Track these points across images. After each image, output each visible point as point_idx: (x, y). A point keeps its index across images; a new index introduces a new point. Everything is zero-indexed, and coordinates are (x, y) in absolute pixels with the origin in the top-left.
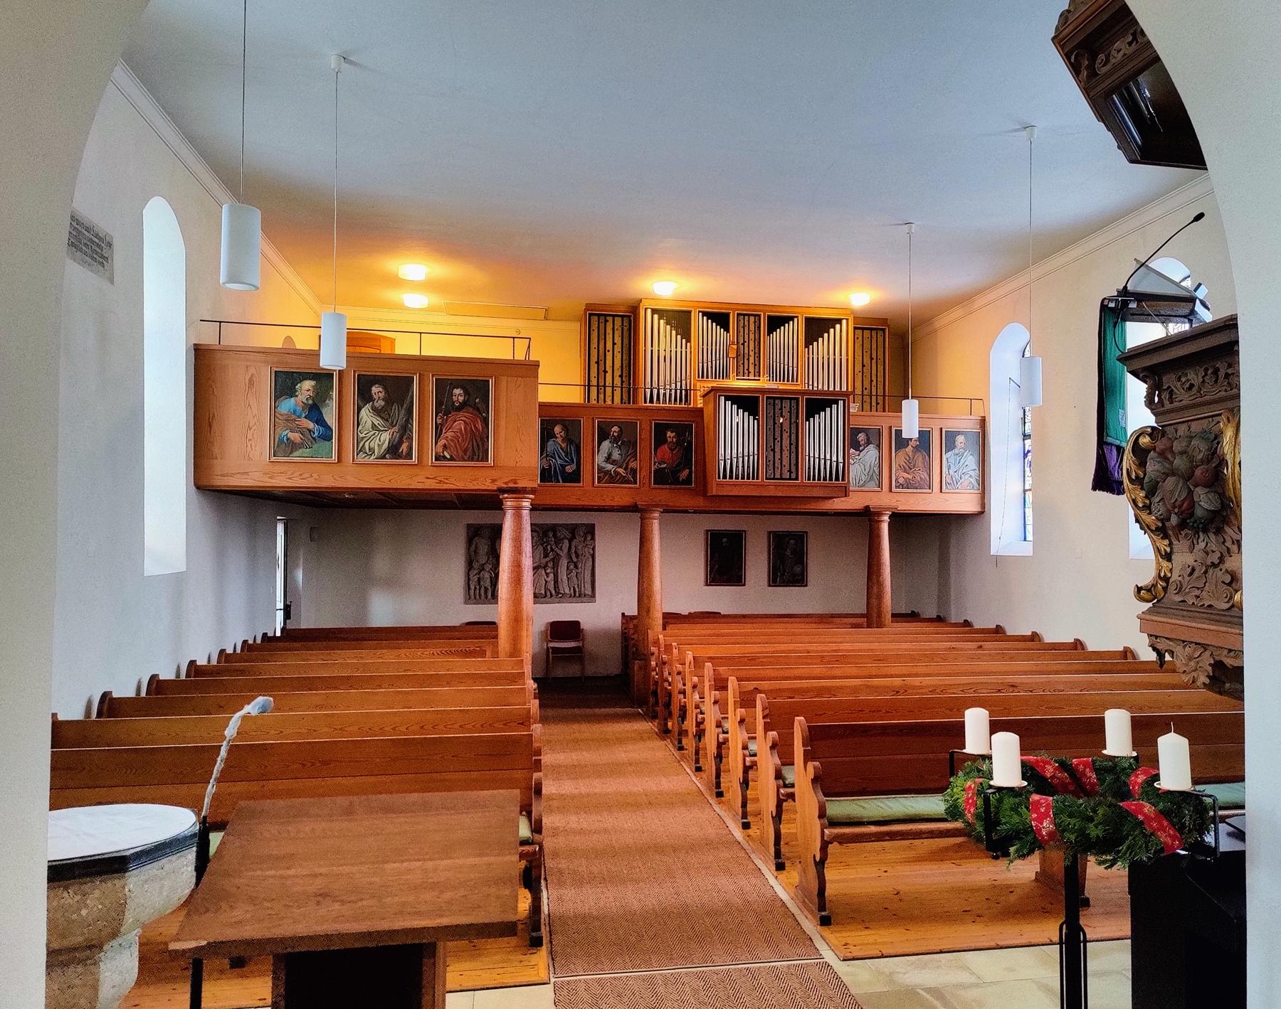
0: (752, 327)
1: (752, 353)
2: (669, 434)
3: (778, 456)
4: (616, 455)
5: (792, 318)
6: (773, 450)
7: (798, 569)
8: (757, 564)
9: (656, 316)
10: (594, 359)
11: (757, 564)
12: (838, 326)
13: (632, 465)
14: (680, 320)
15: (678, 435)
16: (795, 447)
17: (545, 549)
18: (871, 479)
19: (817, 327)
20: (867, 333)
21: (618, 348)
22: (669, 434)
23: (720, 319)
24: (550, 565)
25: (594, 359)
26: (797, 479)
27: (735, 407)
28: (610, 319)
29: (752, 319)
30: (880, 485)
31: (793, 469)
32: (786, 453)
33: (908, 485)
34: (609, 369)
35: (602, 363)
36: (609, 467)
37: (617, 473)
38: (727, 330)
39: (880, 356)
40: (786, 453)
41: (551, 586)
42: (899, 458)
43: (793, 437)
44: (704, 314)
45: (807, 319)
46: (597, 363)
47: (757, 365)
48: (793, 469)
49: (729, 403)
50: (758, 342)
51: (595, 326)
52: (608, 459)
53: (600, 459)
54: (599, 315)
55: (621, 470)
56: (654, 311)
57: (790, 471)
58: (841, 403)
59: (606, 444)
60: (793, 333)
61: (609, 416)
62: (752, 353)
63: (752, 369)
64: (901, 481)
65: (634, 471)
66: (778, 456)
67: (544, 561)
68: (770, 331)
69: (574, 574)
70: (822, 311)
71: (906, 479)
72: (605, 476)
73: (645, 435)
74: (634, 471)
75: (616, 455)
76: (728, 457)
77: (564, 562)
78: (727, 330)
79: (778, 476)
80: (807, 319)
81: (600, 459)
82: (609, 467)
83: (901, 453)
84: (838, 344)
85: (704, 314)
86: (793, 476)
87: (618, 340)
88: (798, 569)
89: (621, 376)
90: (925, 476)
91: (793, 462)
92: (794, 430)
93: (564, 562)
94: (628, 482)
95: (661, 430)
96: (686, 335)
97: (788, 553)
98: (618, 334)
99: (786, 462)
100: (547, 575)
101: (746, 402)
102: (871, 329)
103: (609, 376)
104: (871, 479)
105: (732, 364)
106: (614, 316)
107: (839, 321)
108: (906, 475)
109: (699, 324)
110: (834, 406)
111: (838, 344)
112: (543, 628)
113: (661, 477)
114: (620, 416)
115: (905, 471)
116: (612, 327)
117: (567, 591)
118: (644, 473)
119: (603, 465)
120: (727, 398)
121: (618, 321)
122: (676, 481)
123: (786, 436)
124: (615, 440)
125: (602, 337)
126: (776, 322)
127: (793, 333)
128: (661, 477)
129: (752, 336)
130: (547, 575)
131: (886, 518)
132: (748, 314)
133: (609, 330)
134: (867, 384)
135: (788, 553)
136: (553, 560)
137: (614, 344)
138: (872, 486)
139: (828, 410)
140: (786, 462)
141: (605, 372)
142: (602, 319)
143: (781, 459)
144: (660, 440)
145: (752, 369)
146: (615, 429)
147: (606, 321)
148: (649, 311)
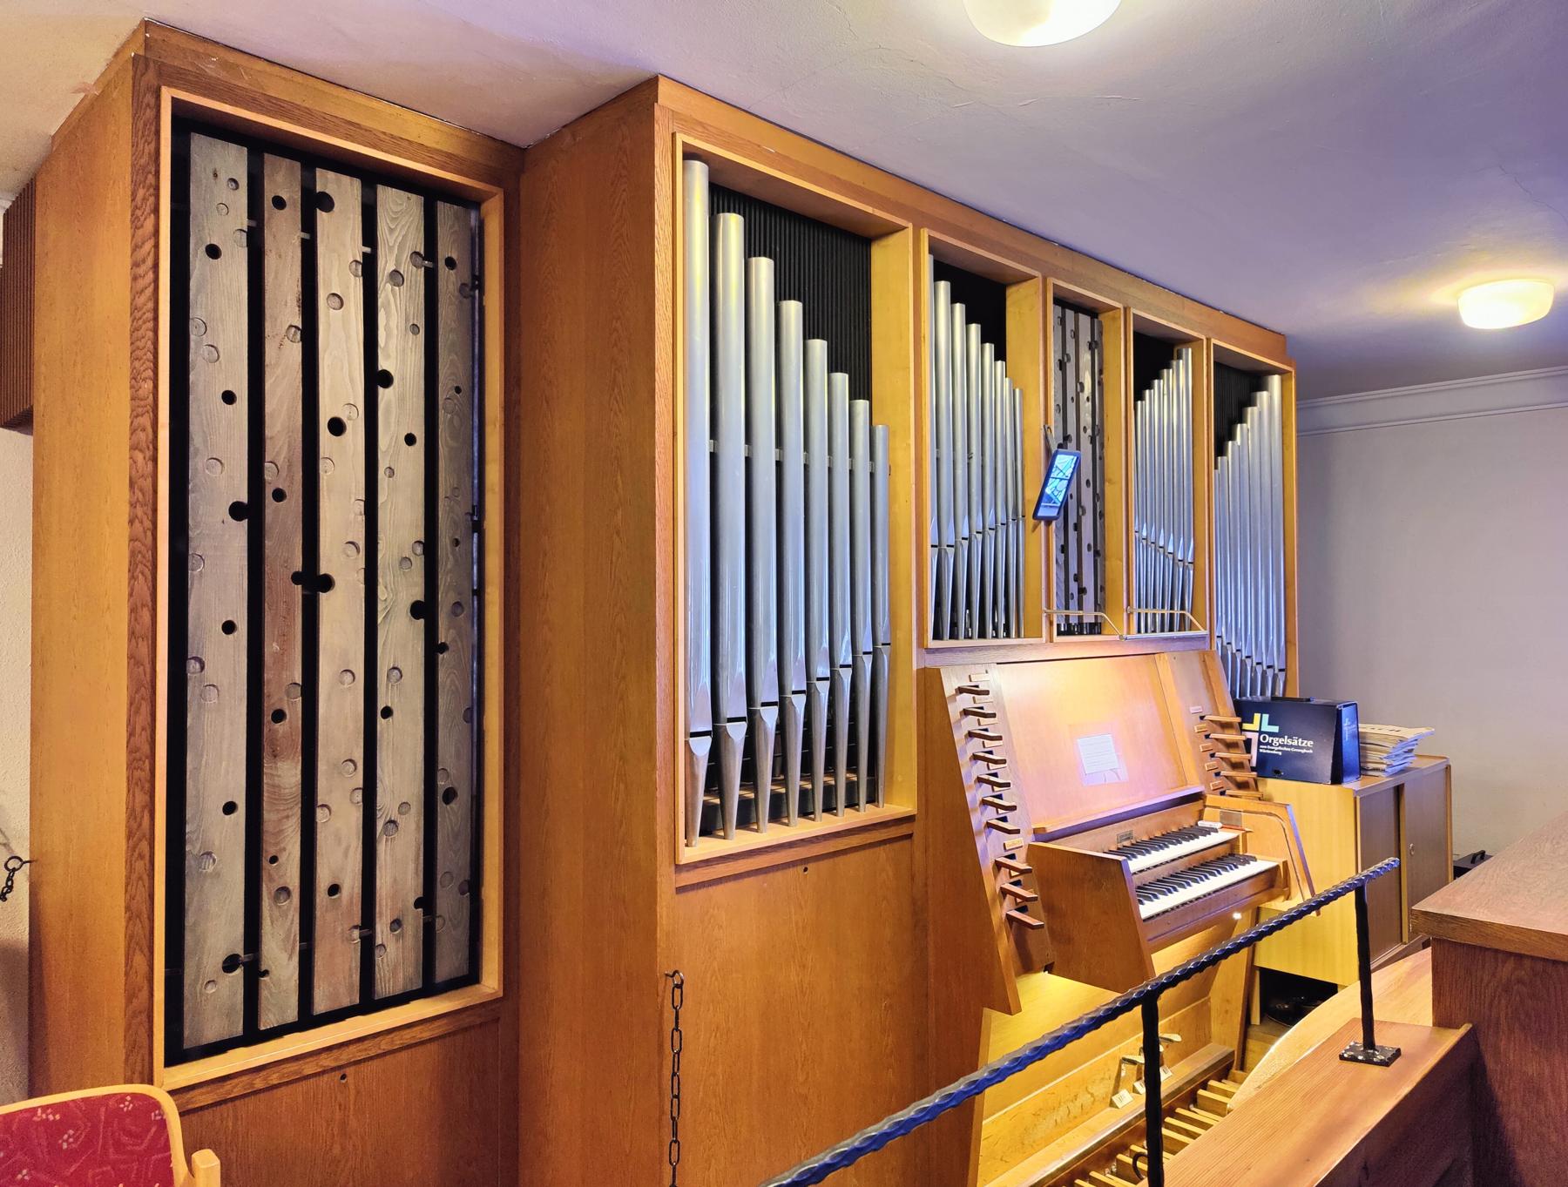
9: (733, 224)
21: (401, 409)
25: (221, 477)
34: (339, 556)
35: (283, 518)
51: (221, 215)
54: (261, 145)
87: (401, 354)
98: (399, 309)
103: (340, 615)
105: (1038, 551)
106: (372, 175)
121: (400, 217)
133: (338, 274)
137: (376, 379)
141: (314, 582)
147: (314, 203)
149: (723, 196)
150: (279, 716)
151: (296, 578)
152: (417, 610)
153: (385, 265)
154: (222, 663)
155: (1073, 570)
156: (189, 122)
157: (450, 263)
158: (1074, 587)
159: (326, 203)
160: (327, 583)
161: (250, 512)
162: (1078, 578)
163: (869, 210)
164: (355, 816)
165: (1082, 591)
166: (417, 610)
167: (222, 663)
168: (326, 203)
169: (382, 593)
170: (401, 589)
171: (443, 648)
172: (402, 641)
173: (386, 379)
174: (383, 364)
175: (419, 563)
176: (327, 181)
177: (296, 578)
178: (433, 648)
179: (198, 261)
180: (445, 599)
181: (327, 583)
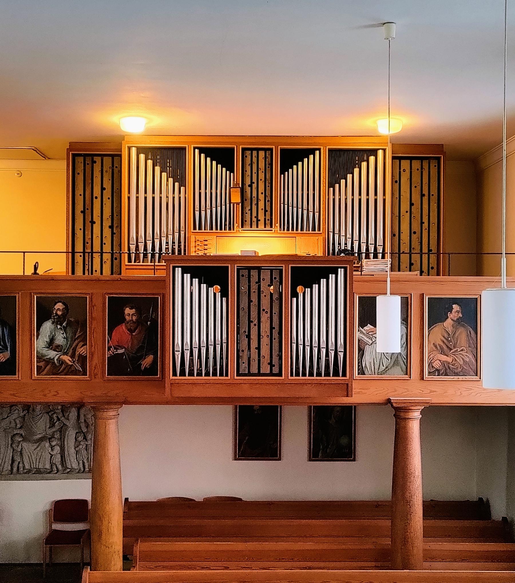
0: (262, 165)
1: (261, 197)
2: (127, 311)
3: (254, 344)
4: (60, 339)
5: (312, 151)
6: (249, 336)
7: (344, 441)
8: (295, 433)
10: (80, 207)
11: (295, 433)
12: (372, 159)
13: (81, 350)
14: (170, 158)
15: (139, 312)
16: (278, 332)
17: (51, 418)
18: (396, 363)
19: (344, 160)
20: (405, 164)
22: (127, 311)
23: (221, 155)
24: (57, 436)
25: (80, 207)
26: (280, 374)
27: (196, 281)
28: (98, 159)
29: (262, 154)
30: (407, 372)
31: (275, 361)
32: (265, 341)
33: (446, 370)
35: (88, 212)
36: (52, 354)
37: (62, 362)
38: (230, 168)
39: (434, 191)
40: (265, 341)
41: (57, 459)
42: (436, 335)
43: (276, 318)
44: (202, 150)
45: (330, 151)
46: (83, 212)
47: (269, 210)
48: (275, 361)
49: (187, 277)
50: (269, 182)
52: (51, 344)
53: (40, 344)
54: (85, 156)
55: (66, 358)
56: (140, 150)
57: (271, 365)
58: (341, 272)
59: (48, 326)
60: (315, 167)
61: (49, 290)
62: (261, 197)
63: (261, 217)
64: (437, 365)
65: (83, 360)
66: (254, 344)
67: (50, 432)
68: (284, 169)
69: (82, 447)
70: (345, 140)
71: (443, 363)
72: (47, 366)
73: (98, 314)
74: (83, 360)
75: (60, 339)
76: (187, 346)
77: (71, 434)
78: (232, 170)
79: (254, 369)
80: (330, 151)
81: (40, 344)
82: (52, 354)
83: (438, 329)
84: (374, 177)
85: (202, 150)
86: (276, 370)
88: (344, 441)
89: (111, 227)
90: (469, 358)
91: (275, 353)
92: (276, 310)
93: (71, 434)
94: (75, 372)
95: (117, 306)
96: (179, 177)
97: (332, 421)
99: (265, 350)
100: (52, 448)
101: (212, 273)
102: (422, 159)
103: (97, 228)
104: (396, 363)
107: (374, 152)
108: (444, 358)
109: (197, 164)
110: (332, 277)
111: (374, 177)
112: (48, 507)
113: (117, 366)
114: (65, 290)
115: (443, 352)
116: (93, 166)
117: (75, 466)
118: (96, 361)
119: (45, 351)
120: (185, 270)
122: (137, 371)
123: (265, 317)
124: (58, 321)
125: (89, 181)
126: (293, 156)
127: (315, 167)
128: (117, 366)
129: (262, 176)
130: (52, 448)
131: (416, 414)
132: (257, 148)
134: (416, 227)
135: (332, 421)
136: (60, 430)
137: (103, 189)
138: (397, 372)
139: (323, 281)
140: (265, 350)
141: (93, 222)
142: (88, 160)
143: (259, 348)
144: (116, 318)
145: (261, 217)
146: (59, 306)
148: (134, 151)
149: (140, 150)
150: (87, 243)
151: (90, 222)
152: (110, 227)
153: (104, 170)
154: (79, 234)
155: (254, 214)
156: (74, 155)
157: (116, 167)
158: (254, 219)
159: (95, 162)
160: (95, 223)
161: (83, 212)
162: (257, 217)
163: (175, 145)
164: (99, 260)
165: (258, 220)
166: (110, 227)
167: (79, 234)
168: (95, 162)
169: (104, 224)
170: (107, 223)
171: (115, 234)
172: (107, 232)
173: (105, 189)
174: (104, 187)
175: (110, 219)
176: (95, 158)
177: (90, 222)
178: (113, 234)
179: (76, 175)
180: (115, 225)
181: (95, 223)
